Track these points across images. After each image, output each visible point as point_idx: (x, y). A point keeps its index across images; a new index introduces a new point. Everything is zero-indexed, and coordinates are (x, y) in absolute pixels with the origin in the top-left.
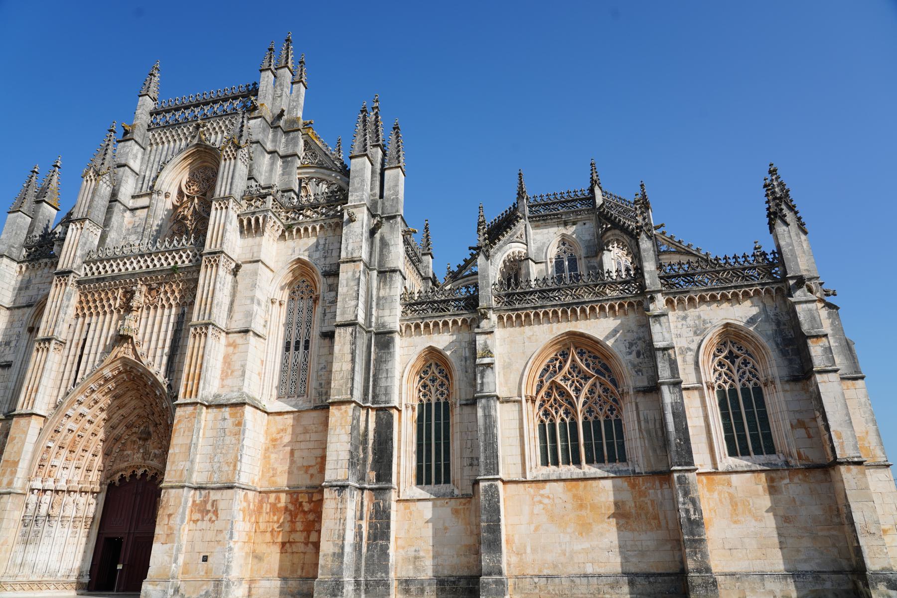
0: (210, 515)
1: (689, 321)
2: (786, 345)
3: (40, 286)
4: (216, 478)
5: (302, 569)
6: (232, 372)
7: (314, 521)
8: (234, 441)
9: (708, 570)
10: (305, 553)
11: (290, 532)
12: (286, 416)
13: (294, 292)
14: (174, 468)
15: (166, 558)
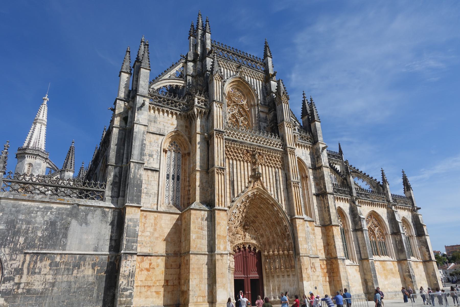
3: (165, 124)
15: (310, 288)
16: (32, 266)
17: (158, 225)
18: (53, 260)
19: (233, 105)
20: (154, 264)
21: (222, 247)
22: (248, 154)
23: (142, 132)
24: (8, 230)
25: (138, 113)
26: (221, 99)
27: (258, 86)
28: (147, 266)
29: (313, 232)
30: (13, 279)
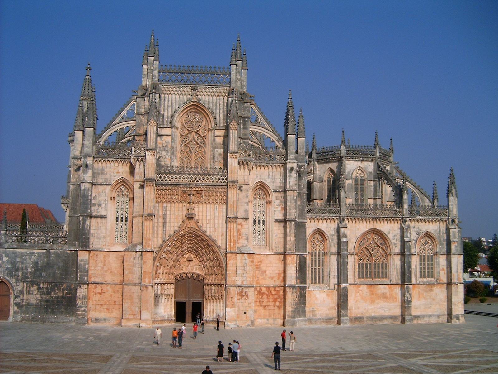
0: (245, 297)
1: (415, 229)
2: (444, 241)
3: (112, 174)
4: (245, 283)
5: (274, 315)
6: (242, 237)
7: (277, 298)
8: (251, 269)
9: (411, 315)
10: (274, 310)
11: (268, 302)
12: (261, 255)
13: (255, 195)
14: (230, 279)
15: (233, 313)
16: (28, 289)
17: (107, 262)
18: (39, 285)
19: (188, 134)
20: (105, 290)
21: (147, 280)
22: (185, 195)
23: (87, 189)
24: (13, 268)
25: (84, 174)
26: (154, 146)
27: (218, 105)
28: (100, 291)
29: (251, 264)
30: (20, 297)
